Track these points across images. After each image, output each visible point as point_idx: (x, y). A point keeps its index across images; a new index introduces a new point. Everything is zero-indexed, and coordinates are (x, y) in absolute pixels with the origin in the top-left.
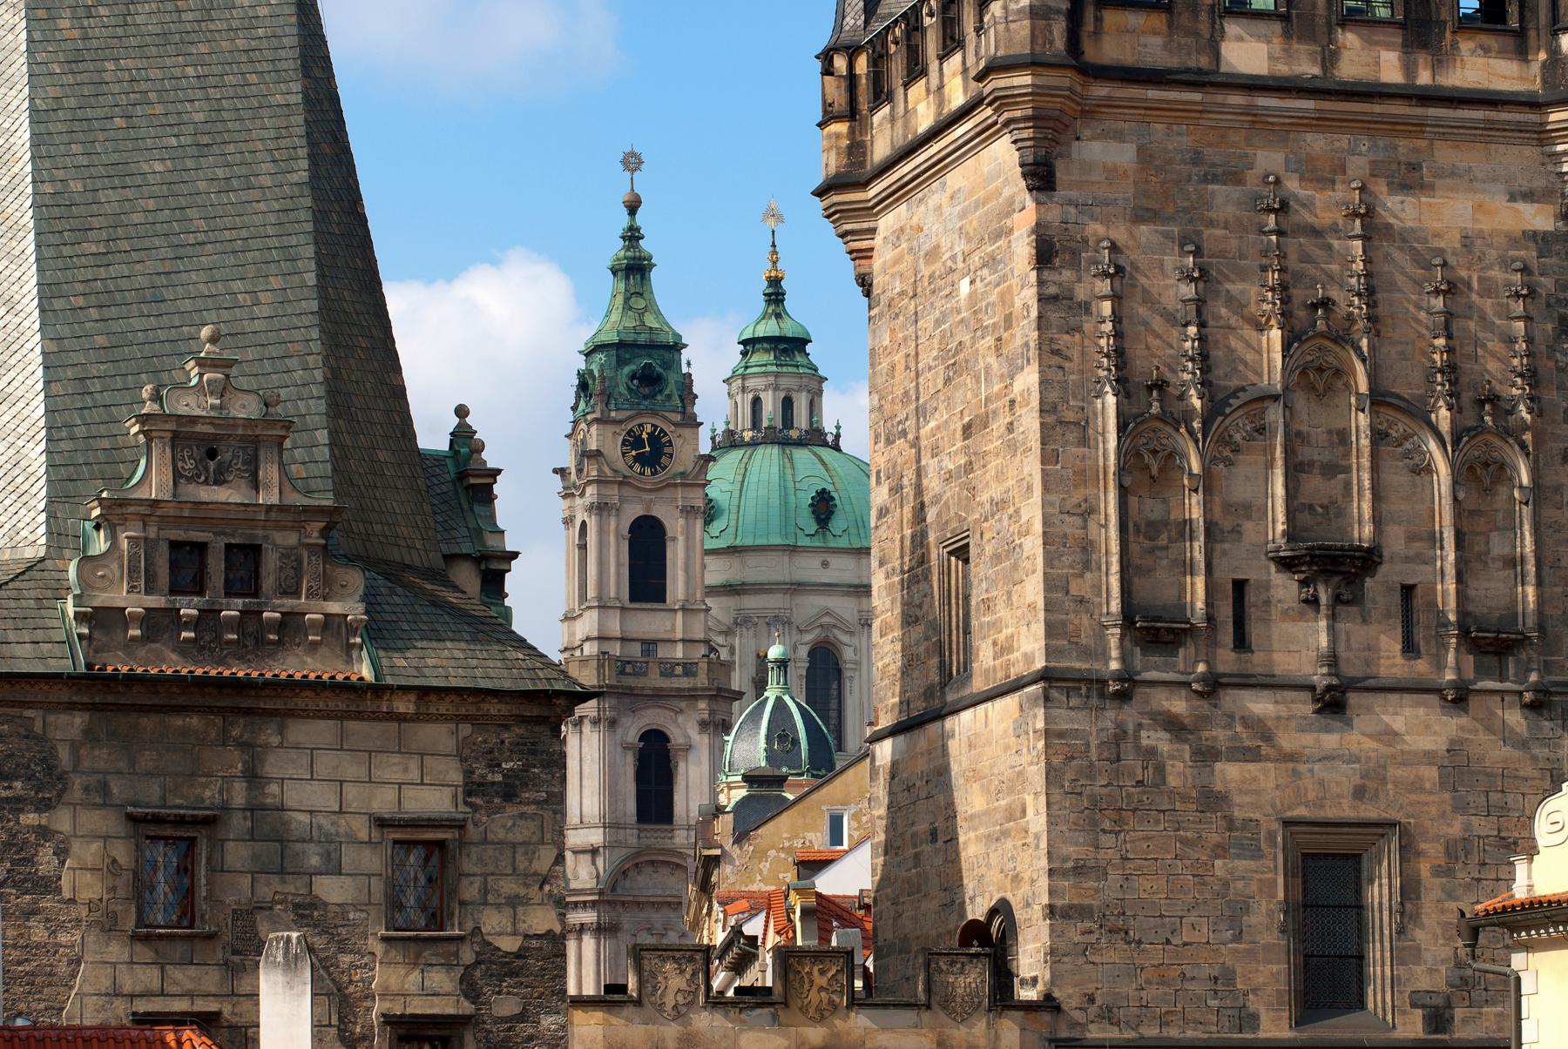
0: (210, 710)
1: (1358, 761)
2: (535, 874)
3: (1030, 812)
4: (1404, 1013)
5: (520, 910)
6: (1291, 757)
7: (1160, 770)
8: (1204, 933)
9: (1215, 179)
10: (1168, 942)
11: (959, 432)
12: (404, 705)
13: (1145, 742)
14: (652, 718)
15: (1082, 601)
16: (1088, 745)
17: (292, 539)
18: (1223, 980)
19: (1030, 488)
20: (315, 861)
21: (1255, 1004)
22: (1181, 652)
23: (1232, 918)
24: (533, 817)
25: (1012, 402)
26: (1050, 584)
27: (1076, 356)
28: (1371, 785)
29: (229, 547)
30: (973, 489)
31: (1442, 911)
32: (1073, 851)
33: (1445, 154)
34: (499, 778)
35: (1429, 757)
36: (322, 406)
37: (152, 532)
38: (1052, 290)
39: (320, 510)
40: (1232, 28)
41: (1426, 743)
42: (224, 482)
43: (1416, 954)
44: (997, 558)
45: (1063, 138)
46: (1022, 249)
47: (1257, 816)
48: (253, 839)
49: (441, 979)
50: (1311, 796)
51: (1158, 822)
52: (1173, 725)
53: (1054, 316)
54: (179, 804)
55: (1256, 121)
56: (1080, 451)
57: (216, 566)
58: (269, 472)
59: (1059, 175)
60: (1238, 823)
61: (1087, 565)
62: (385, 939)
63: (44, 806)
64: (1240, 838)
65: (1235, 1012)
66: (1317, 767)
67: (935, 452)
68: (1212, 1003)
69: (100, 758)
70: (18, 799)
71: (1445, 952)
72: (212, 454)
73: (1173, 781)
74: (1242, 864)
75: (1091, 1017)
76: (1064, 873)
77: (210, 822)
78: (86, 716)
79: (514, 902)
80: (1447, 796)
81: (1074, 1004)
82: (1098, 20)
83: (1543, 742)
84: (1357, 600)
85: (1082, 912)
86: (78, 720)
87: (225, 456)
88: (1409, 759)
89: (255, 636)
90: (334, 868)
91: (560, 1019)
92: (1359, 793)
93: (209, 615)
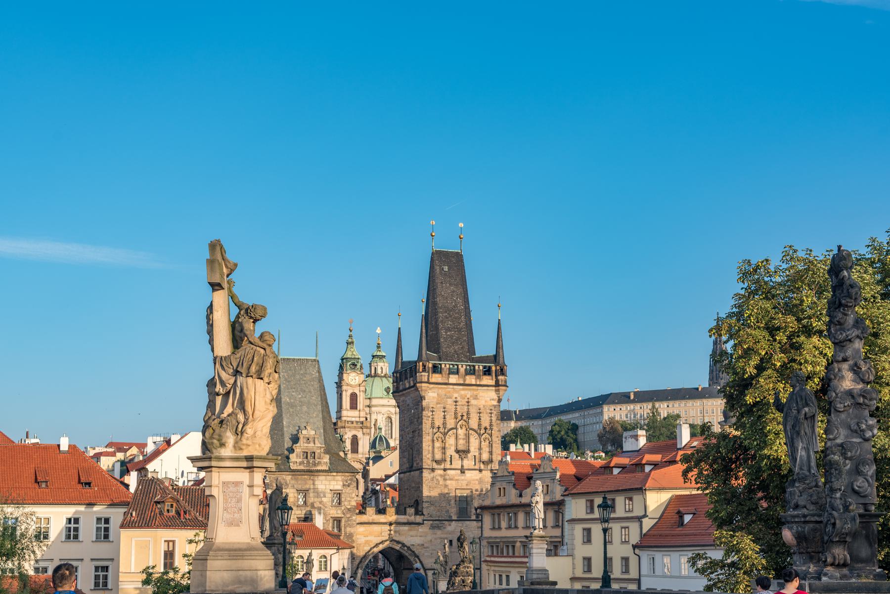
14: (354, 432)
33: (481, 394)
52: (441, 476)
54: (304, 488)
58: (316, 442)
69: (293, 482)
89: (315, 465)
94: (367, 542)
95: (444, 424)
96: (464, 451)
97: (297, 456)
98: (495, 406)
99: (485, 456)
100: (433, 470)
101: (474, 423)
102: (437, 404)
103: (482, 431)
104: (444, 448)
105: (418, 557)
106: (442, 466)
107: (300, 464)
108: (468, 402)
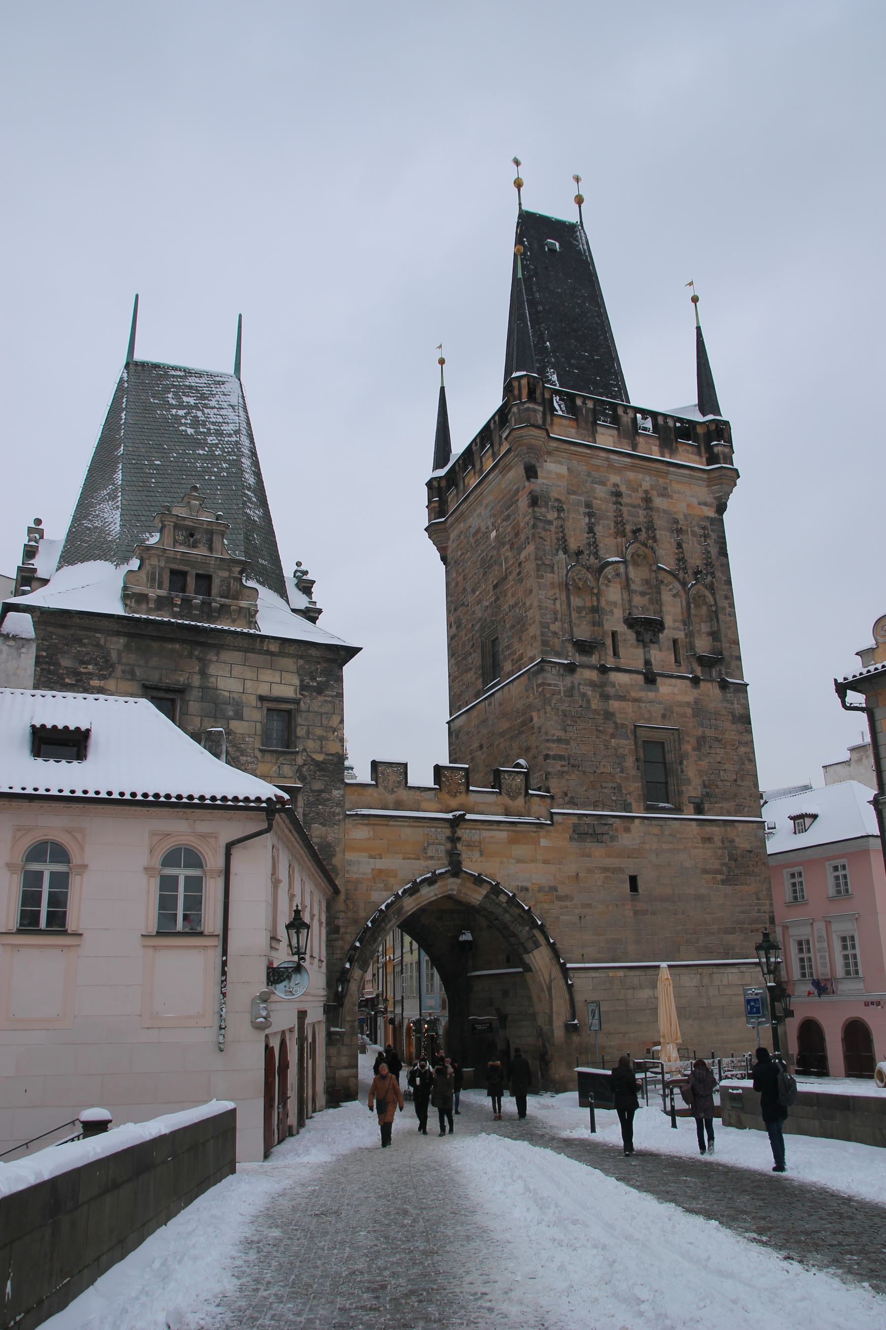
0: (183, 641)
1: (662, 704)
2: (331, 727)
3: (535, 719)
5: (324, 742)
6: (636, 700)
7: (588, 701)
8: (608, 769)
9: (596, 483)
10: (595, 772)
11: (491, 590)
12: (274, 647)
13: (582, 691)
15: (555, 633)
17: (226, 574)
19: (531, 591)
20: (231, 713)
21: (630, 799)
23: (620, 764)
24: (330, 702)
25: (520, 564)
26: (544, 625)
27: (549, 540)
29: (198, 576)
30: (499, 607)
31: (697, 765)
33: (676, 486)
34: (315, 684)
36: (241, 537)
37: (162, 564)
38: (538, 514)
39: (239, 562)
40: (598, 428)
42: (197, 547)
43: (689, 782)
44: (513, 627)
46: (523, 502)
48: (202, 701)
49: (287, 770)
50: (646, 716)
52: (592, 684)
53: (540, 525)
56: (551, 575)
57: (191, 582)
58: (217, 544)
61: (556, 619)
62: (261, 750)
63: (104, 678)
66: (648, 705)
67: (479, 602)
69: (131, 658)
70: (90, 674)
72: (192, 535)
73: (593, 707)
74: (624, 742)
76: (553, 741)
77: (182, 691)
78: (126, 639)
79: (321, 739)
82: (552, 420)
85: (561, 758)
86: (122, 641)
87: (198, 536)
88: (680, 704)
89: (207, 612)
90: (239, 716)
91: (341, 792)
92: (664, 716)
93: (186, 601)
94: (379, 874)
96: (648, 622)
97: (151, 578)
98: (712, 520)
99: (703, 645)
100: (571, 668)
102: (569, 493)
105: (542, 928)
106: (594, 659)
107: (162, 603)
108: (647, 500)
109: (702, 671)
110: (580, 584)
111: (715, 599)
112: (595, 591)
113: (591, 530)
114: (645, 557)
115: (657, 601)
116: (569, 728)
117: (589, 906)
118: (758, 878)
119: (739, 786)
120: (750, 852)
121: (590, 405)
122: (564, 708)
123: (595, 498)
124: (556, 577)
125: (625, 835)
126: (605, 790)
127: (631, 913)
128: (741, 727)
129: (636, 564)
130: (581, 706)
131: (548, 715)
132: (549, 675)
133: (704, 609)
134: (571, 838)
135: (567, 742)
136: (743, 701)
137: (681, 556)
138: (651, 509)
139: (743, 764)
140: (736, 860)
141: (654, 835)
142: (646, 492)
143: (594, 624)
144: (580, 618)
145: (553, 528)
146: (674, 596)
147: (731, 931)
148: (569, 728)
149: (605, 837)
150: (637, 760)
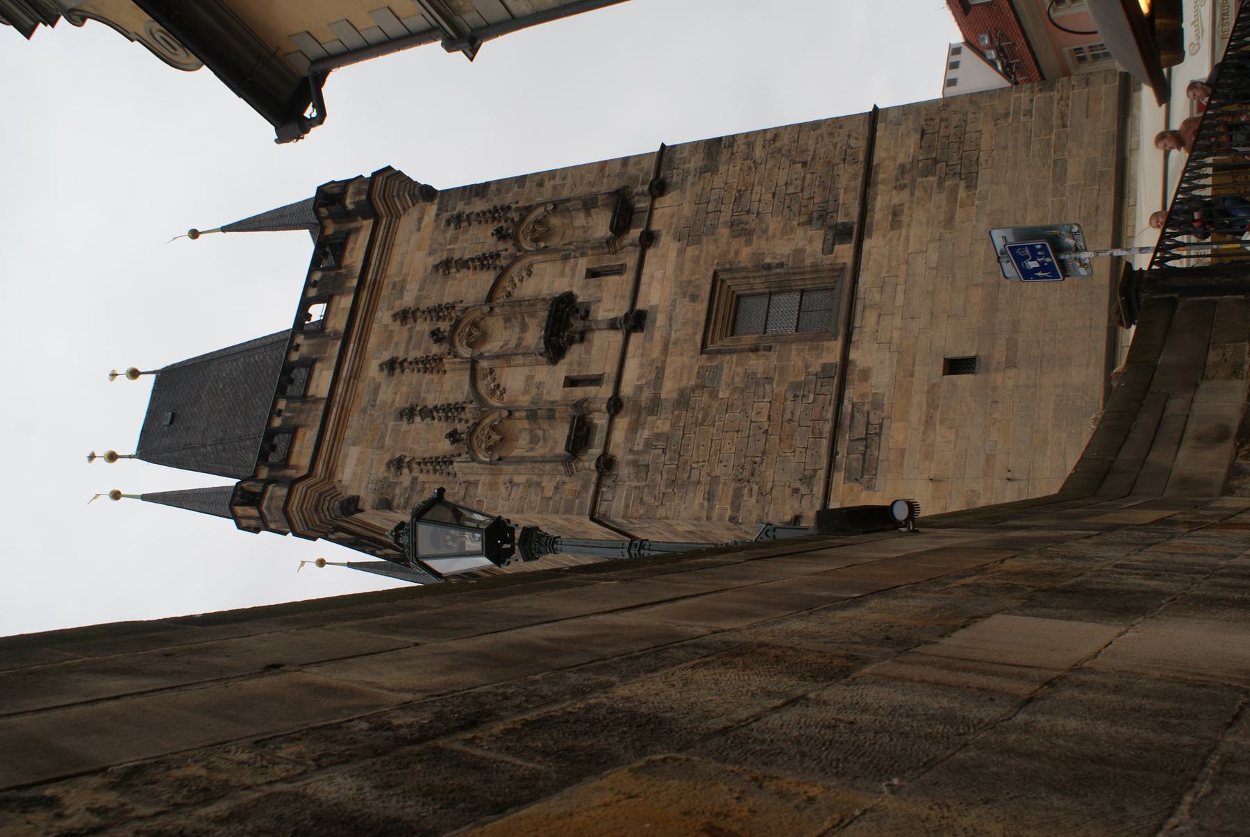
1: (675, 300)
3: (686, 528)
4: (836, 258)
7: (658, 436)
9: (375, 401)
10: (766, 432)
13: (641, 447)
15: (557, 488)
16: (635, 487)
18: (797, 390)
21: (816, 367)
22: (596, 421)
23: (757, 384)
28: (691, 290)
31: (774, 236)
32: (697, 499)
33: (392, 269)
35: (681, 252)
38: (402, 500)
40: (311, 391)
41: (672, 255)
43: (799, 252)
45: (339, 489)
47: (696, 368)
50: (690, 331)
51: (689, 439)
52: (634, 428)
55: (355, 375)
56: (480, 486)
59: (354, 494)
60: (699, 382)
64: (706, 383)
65: (819, 381)
66: (674, 328)
68: (811, 397)
71: (800, 232)
75: (808, 491)
76: (711, 508)
80: (705, 239)
81: (796, 505)
82: (294, 467)
83: (684, 180)
84: (589, 303)
85: (737, 495)
88: (680, 267)
92: (694, 298)
95: (450, 411)
98: (441, 209)
99: (601, 224)
100: (606, 464)
101: (469, 288)
102: (382, 447)
103: (506, 247)
104: (532, 415)
106: (600, 420)
108: (404, 316)
109: (638, 227)
110: (496, 437)
111: (539, 205)
112: (505, 413)
113: (427, 413)
114: (475, 324)
115: (533, 302)
116: (694, 478)
117: (989, 458)
118: (970, 116)
119: (813, 158)
120: (923, 133)
121: (282, 404)
122: (663, 483)
123: (393, 402)
124: (483, 478)
125: (873, 381)
126: (797, 413)
127: (1011, 373)
128: (725, 154)
129: (484, 337)
130: (664, 451)
131: (670, 514)
132: (614, 504)
133: (555, 221)
134: (868, 488)
135: (715, 480)
136: (686, 153)
137: (478, 263)
138: (414, 313)
139: (780, 150)
140: (936, 161)
141: (878, 324)
142: (395, 316)
143: (551, 416)
144: (545, 440)
145: (422, 478)
146: (530, 274)
147: (1060, 167)
148: (694, 478)
149: (874, 419)
150: (755, 349)
